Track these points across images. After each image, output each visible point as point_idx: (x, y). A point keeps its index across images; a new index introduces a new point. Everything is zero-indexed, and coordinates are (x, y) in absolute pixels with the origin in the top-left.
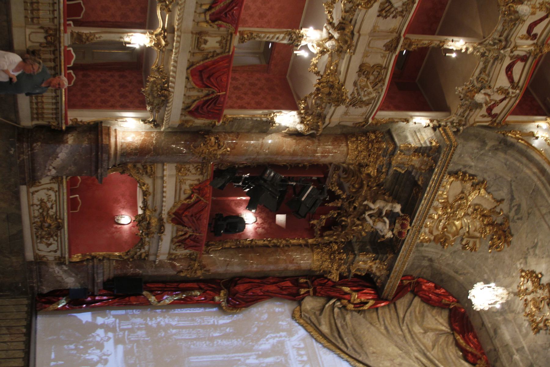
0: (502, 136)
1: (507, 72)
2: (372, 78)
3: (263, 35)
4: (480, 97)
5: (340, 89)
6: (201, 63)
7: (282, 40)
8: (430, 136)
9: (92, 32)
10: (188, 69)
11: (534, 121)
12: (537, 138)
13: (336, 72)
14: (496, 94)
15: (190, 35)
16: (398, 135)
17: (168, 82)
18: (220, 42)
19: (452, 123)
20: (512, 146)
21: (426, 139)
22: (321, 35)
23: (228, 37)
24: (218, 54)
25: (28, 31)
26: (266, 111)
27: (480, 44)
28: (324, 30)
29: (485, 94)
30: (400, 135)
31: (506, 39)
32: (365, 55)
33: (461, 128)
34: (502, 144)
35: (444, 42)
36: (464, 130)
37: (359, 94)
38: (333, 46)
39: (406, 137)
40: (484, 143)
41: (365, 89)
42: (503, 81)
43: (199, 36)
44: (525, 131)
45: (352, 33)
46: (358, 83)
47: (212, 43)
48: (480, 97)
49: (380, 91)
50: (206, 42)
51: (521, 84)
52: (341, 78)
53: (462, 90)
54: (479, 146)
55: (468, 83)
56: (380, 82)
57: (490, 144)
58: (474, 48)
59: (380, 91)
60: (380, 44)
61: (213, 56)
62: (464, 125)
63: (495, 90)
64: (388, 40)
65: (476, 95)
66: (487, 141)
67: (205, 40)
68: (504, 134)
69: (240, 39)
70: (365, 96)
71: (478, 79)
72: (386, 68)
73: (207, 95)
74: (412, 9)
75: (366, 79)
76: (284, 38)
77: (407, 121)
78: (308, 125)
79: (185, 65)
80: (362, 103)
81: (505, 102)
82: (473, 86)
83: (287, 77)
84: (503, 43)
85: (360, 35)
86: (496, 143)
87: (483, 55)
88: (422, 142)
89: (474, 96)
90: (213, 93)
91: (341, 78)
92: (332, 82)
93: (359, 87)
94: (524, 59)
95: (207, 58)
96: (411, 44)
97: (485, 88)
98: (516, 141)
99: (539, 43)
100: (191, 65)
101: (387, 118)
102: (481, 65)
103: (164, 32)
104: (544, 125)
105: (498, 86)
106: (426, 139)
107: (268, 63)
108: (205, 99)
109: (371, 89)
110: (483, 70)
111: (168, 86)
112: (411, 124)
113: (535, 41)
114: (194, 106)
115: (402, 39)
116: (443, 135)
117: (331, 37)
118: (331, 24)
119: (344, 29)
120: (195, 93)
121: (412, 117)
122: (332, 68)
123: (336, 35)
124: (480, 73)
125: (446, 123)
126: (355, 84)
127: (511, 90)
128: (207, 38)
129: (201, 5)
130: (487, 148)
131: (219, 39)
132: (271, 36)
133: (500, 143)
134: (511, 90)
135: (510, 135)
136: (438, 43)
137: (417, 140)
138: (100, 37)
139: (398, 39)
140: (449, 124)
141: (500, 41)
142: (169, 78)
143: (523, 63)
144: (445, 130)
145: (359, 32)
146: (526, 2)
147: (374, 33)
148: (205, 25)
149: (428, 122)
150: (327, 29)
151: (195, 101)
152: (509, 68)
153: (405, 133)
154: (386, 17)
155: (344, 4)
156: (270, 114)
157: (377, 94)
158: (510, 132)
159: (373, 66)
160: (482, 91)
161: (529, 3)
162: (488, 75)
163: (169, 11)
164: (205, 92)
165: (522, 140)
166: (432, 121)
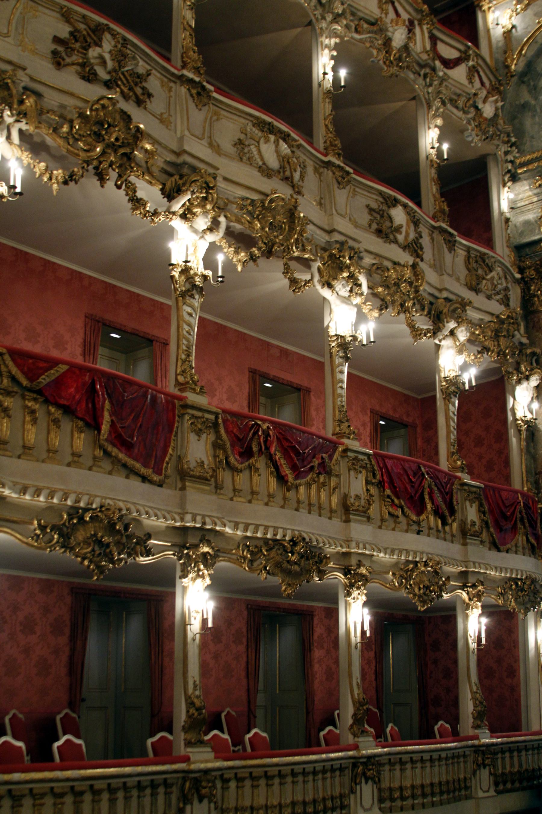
0: (515, 79)
1: (451, 68)
2: (480, 272)
3: (453, 437)
4: (488, 110)
5: (502, 322)
6: (492, 530)
7: (455, 407)
8: (527, 188)
9: (469, 696)
10: (499, 550)
11: (488, 31)
12: (514, 27)
13: (479, 325)
14: (475, 84)
15: (469, 547)
16: (521, 234)
17: (515, 581)
18: (472, 502)
19: (506, 153)
20: (530, 65)
21: (530, 193)
22: (448, 348)
23: (465, 490)
24: (481, 505)
25: (481, 794)
26: (512, 432)
27: (429, 107)
28: (443, 343)
29: (484, 101)
30: (522, 232)
31: (422, 66)
32: (458, 280)
33: (513, 140)
34: (525, 79)
35: (432, 161)
36: (515, 136)
37: (498, 293)
38: (466, 329)
39: (527, 223)
40: (525, 106)
41: (495, 282)
42: (459, 74)
43: (465, 533)
44: (501, 44)
45: (447, 299)
46: (489, 293)
47: (472, 513)
48: (488, 110)
49: (493, 260)
50: (473, 524)
51: (462, 48)
52: (487, 318)
53: (477, 136)
54: (530, 114)
55: (470, 127)
56: (484, 261)
57: (526, 96)
58: (435, 116)
59: (493, 260)
60: (448, 257)
61: (484, 513)
62: (508, 136)
63: (470, 86)
64: (444, 246)
65: (485, 115)
66: (522, 102)
67: (471, 525)
68: (512, 76)
69: (462, 472)
70: (501, 284)
71: (465, 112)
72: (468, 250)
73: (522, 520)
74: (413, 209)
75: (484, 282)
76: (454, 405)
77: (507, 220)
78: (532, 370)
79: (494, 554)
80: (506, 289)
81: (482, 73)
82: (474, 120)
83: (420, 397)
84: (428, 70)
85: (446, 289)
86: (524, 87)
87: (443, 103)
88: (535, 199)
89: (486, 119)
90: (521, 512)
91: (487, 318)
92: (492, 332)
93: (493, 292)
94: (434, 39)
95: (487, 523)
96: (442, 211)
97: (475, 102)
98: (522, 59)
99: (419, 17)
100: (495, 546)
101: (507, 251)
102: (449, 106)
103: (467, 587)
104: (491, 17)
105: (465, 82)
106: (530, 193)
107: (405, 426)
108: (527, 525)
109: (494, 274)
110: (453, 102)
111: (521, 579)
112: (508, 215)
113: (416, 23)
114: (533, 541)
115: (444, 225)
116: (530, 167)
117: (452, 333)
118: (435, 333)
119: (441, 312)
120: (521, 539)
121: (501, 213)
122: (477, 332)
123: (452, 325)
124: (457, 108)
125: (507, 161)
126: (489, 297)
127: (471, 63)
128: (469, 521)
129: (438, 531)
130: (533, 102)
131: (468, 503)
132: (452, 424)
133: (523, 82)
134: (471, 63)
135: (513, 67)
136: (433, 171)
137: (530, 207)
138: (476, 685)
139: (442, 231)
140: (510, 157)
141: (425, 76)
142: (510, 579)
143: (439, 43)
144: (522, 165)
145: (440, 290)
146: (390, 34)
147: (438, 267)
148: (455, 525)
149: (506, 189)
150: (444, 339)
151: (528, 540)
152: (449, 64)
153: (518, 224)
154: (422, 248)
155: (416, 311)
156: (517, 425)
157: (497, 264)
158: (508, 67)
159: (468, 269)
160: (480, 106)
161: (390, 29)
162: (459, 95)
163: (448, 579)
164: (519, 525)
165: (522, 49)
166: (504, 185)
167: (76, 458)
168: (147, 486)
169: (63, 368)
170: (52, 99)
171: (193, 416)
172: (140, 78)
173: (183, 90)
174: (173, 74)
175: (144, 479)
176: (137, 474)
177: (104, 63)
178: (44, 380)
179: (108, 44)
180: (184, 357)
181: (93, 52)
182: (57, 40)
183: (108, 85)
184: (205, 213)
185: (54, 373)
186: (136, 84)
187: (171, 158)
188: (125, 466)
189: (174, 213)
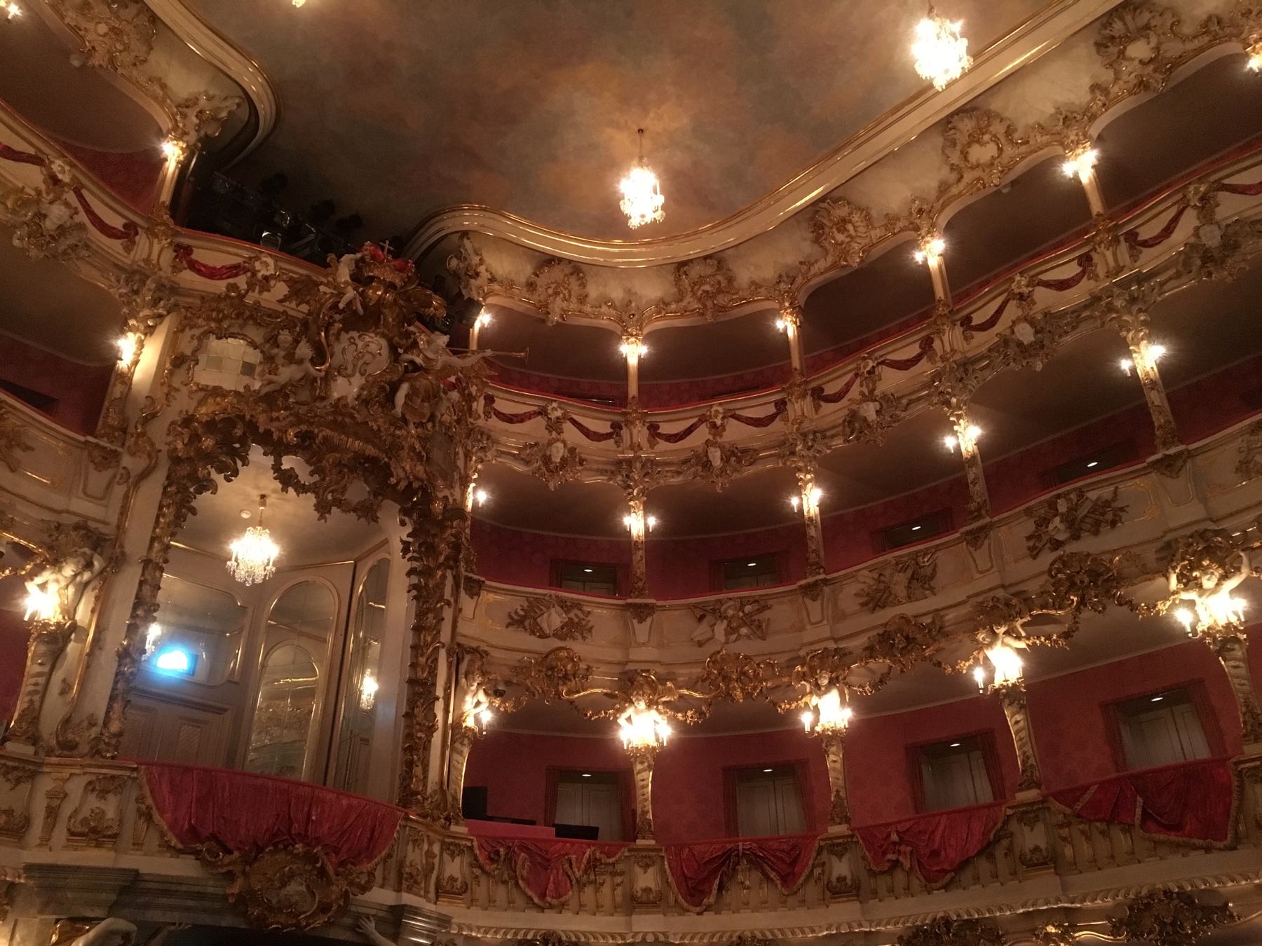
167: (1133, 857)
168: (1214, 856)
169: (1093, 789)
170: (1033, 588)
171: (1249, 769)
172: (1107, 504)
173: (1154, 476)
174: (1144, 468)
175: (1208, 850)
176: (1195, 848)
177: (1059, 530)
178: (1078, 806)
179: (1062, 506)
180: (1244, 709)
181: (1051, 527)
182: (1029, 538)
183: (1076, 537)
184: (1205, 570)
185: (1087, 797)
186: (1103, 514)
187: (1160, 544)
188: (1178, 845)
189: (1174, 593)
